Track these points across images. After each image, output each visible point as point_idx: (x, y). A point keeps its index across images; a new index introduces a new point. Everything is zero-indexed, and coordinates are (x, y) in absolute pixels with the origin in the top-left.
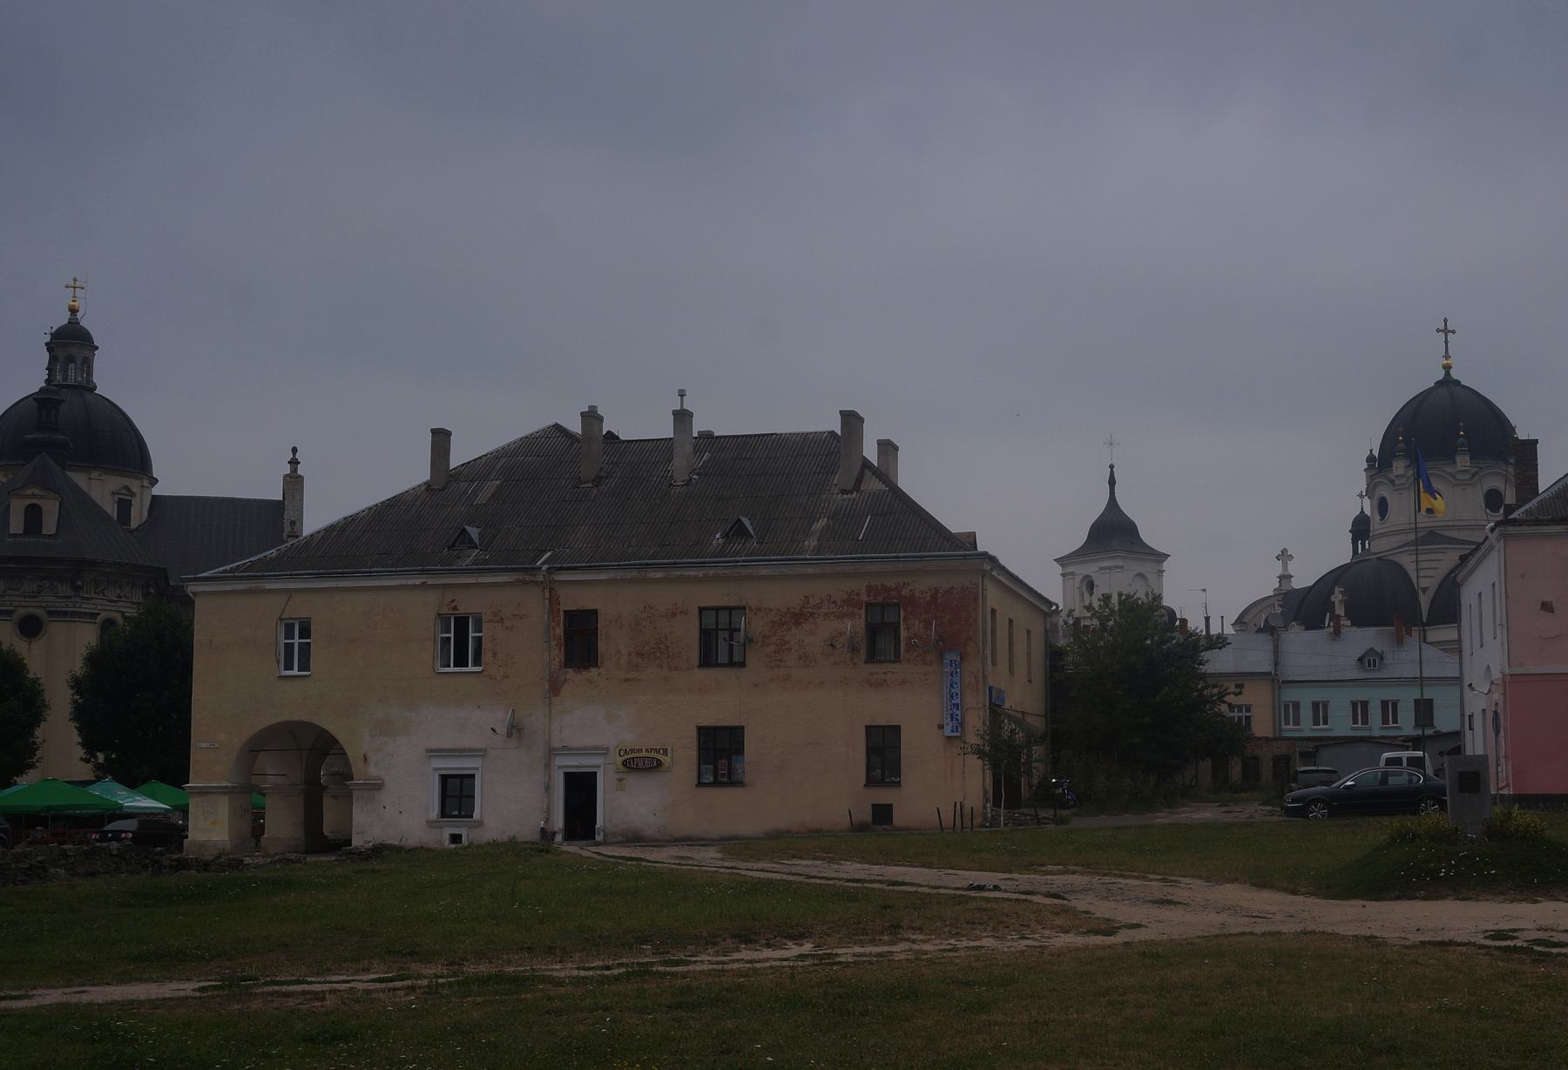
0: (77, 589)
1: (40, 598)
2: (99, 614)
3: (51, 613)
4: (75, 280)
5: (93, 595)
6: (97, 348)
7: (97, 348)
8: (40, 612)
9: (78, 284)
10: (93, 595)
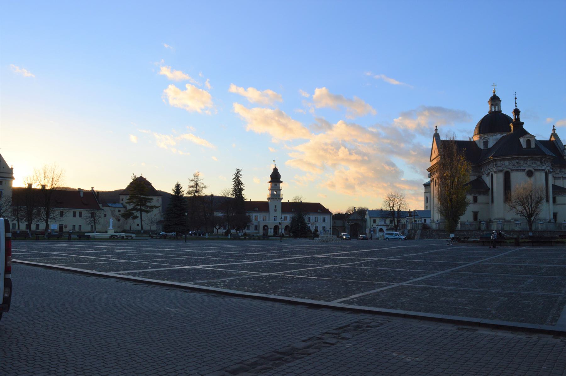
0: (541, 163)
1: (532, 165)
2: (525, 169)
3: (535, 170)
4: (494, 84)
5: (544, 165)
6: (501, 101)
7: (501, 101)
8: (532, 169)
9: (495, 85)
10: (544, 165)
